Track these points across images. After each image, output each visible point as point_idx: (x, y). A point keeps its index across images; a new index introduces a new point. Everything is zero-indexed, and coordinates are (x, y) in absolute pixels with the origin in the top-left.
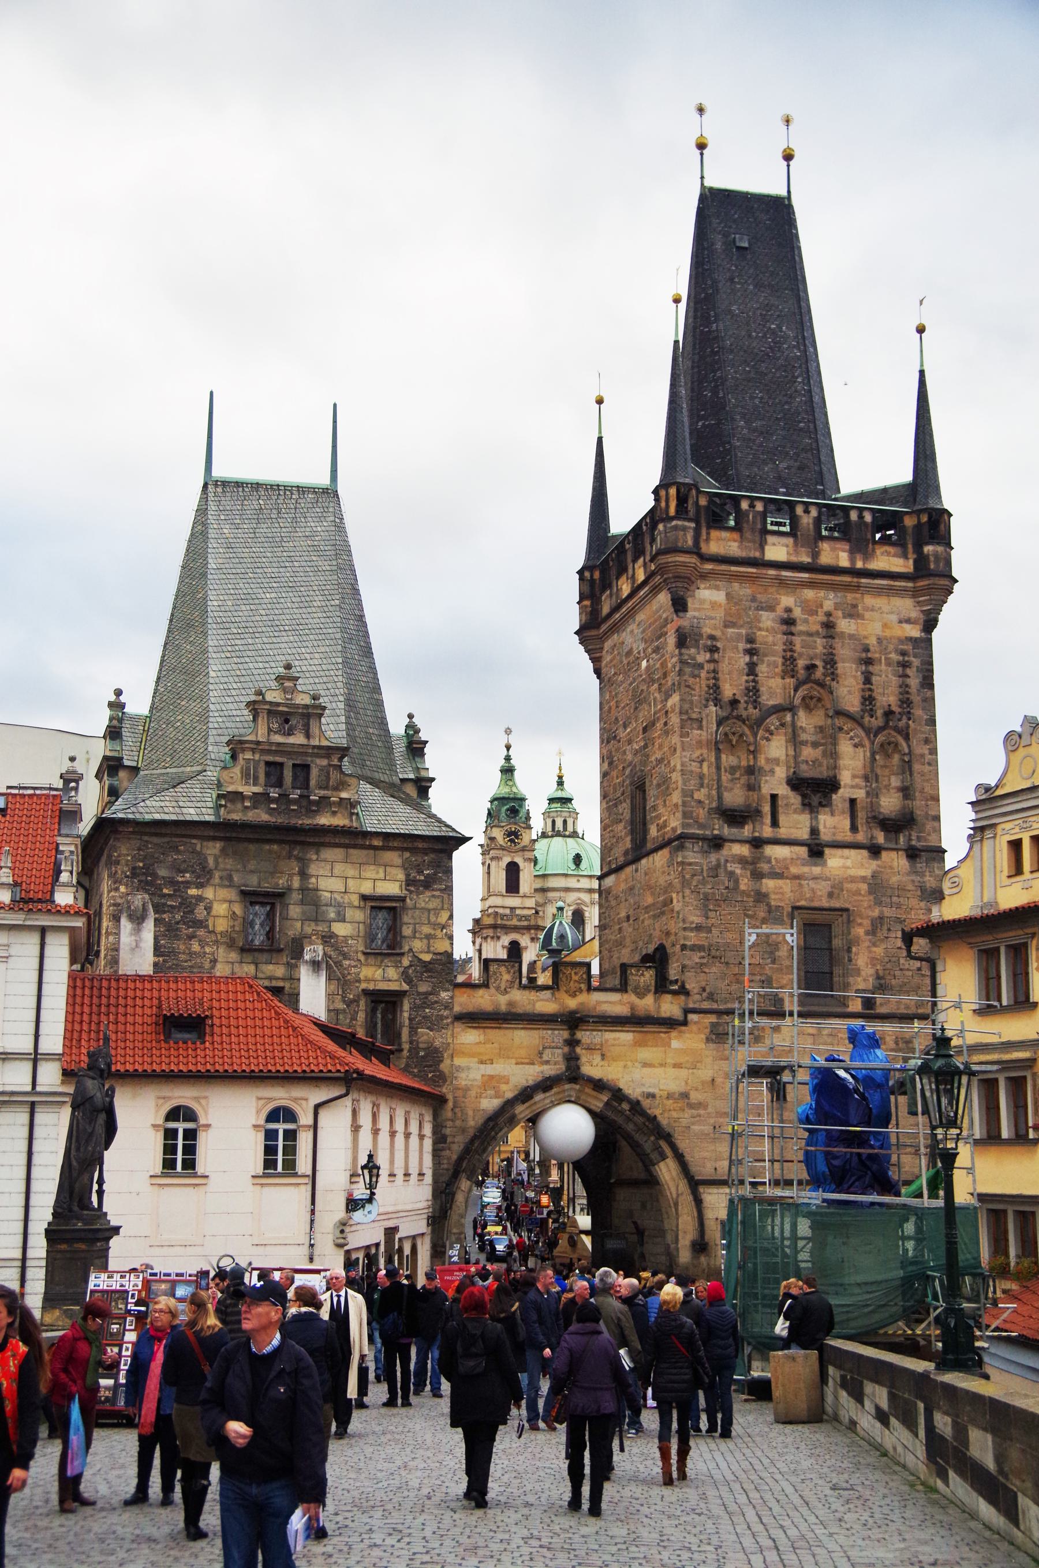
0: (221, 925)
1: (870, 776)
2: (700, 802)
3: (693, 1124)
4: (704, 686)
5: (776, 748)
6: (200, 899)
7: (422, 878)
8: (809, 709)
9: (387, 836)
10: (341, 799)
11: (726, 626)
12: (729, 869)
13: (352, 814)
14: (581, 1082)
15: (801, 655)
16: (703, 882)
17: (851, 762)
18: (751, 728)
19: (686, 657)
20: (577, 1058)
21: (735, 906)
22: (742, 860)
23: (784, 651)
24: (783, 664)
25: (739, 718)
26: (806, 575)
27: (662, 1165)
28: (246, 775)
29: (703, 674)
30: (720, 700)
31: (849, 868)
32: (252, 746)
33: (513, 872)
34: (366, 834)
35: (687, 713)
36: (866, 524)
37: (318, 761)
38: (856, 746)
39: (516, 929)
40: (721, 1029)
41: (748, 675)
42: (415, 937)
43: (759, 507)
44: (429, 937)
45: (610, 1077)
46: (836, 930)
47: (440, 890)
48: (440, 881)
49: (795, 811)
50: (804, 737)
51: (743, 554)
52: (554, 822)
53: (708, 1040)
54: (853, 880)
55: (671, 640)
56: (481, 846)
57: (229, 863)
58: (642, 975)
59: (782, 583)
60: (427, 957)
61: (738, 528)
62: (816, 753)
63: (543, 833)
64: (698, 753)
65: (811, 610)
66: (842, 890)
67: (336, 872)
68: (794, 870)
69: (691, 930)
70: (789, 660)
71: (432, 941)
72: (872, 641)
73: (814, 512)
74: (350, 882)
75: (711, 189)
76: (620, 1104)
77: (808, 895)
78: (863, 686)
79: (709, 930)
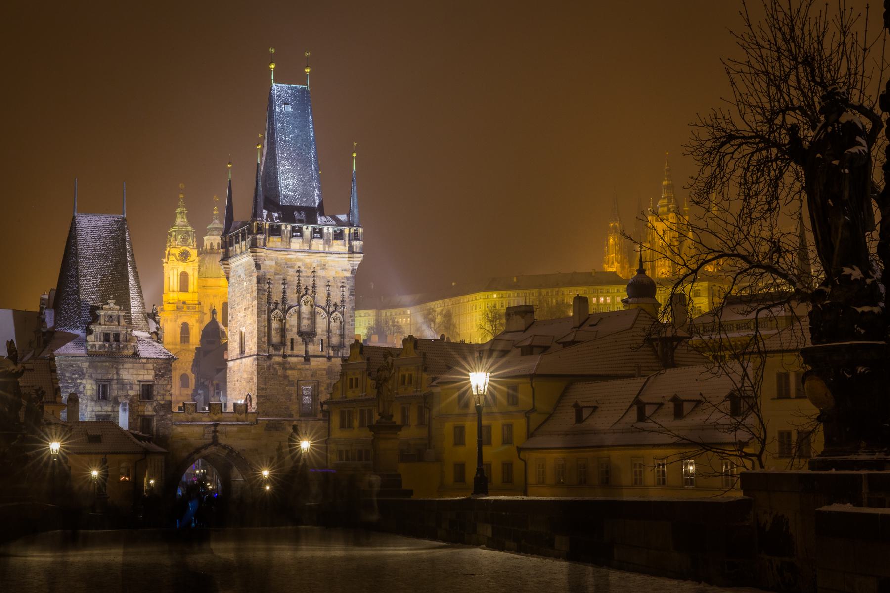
0: (89, 393)
1: (329, 331)
6: (81, 383)
9: (148, 358)
11: (276, 274)
17: (321, 324)
22: (279, 364)
28: (96, 337)
29: (266, 293)
43: (289, 228)
44: (163, 395)
50: (303, 316)
53: (265, 430)
54: (321, 369)
55: (255, 280)
57: (91, 370)
60: (162, 402)
68: (299, 367)
72: (331, 279)
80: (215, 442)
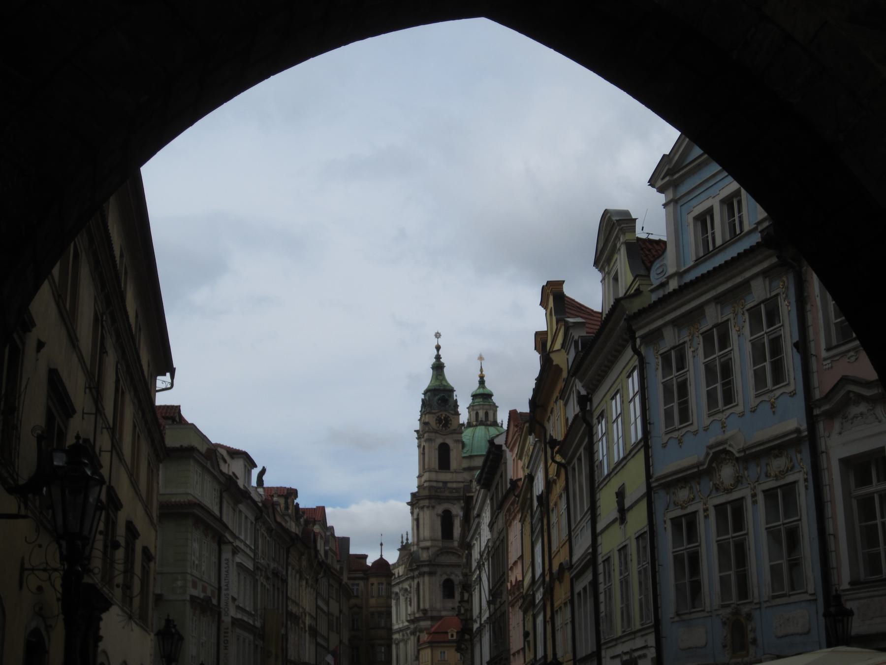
33: (444, 452)
39: (448, 499)
52: (477, 414)
56: (417, 431)
63: (469, 423)
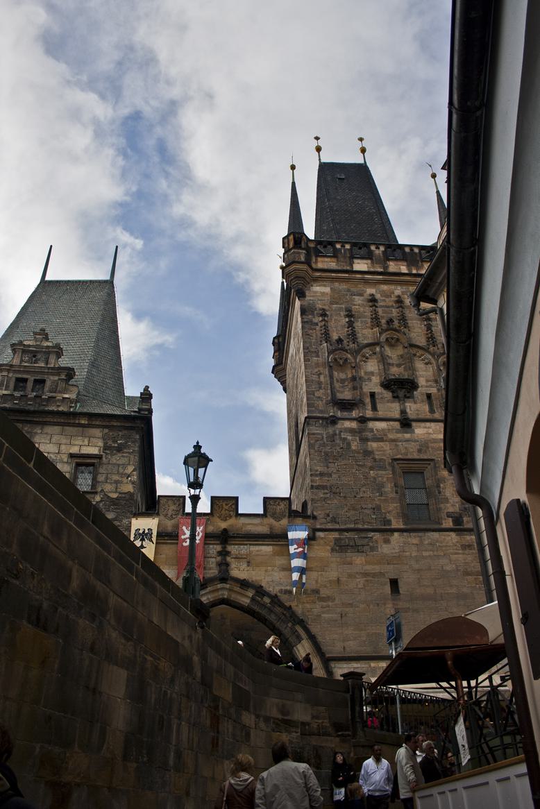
2: (319, 397)
3: (324, 613)
4: (319, 334)
5: (372, 366)
7: (116, 445)
8: (392, 346)
10: (63, 398)
11: (332, 303)
12: (343, 436)
13: (71, 407)
14: (233, 583)
15: (383, 317)
16: (324, 445)
18: (352, 354)
19: (305, 320)
20: (227, 565)
21: (349, 460)
22: (352, 431)
23: (372, 315)
24: (371, 322)
25: (343, 350)
26: (381, 277)
27: (299, 646)
29: (318, 328)
30: (330, 341)
31: (430, 434)
32: (7, 368)
34: (75, 415)
35: (308, 348)
36: (416, 253)
37: (52, 378)
38: (427, 364)
40: (343, 542)
41: (348, 328)
42: (107, 482)
43: (348, 247)
44: (117, 482)
45: (254, 579)
46: (427, 474)
47: (129, 453)
48: (129, 447)
49: (388, 402)
50: (390, 361)
51: (340, 268)
53: (333, 550)
54: (435, 441)
58: (279, 504)
59: (367, 282)
60: (114, 496)
61: (335, 256)
62: (401, 369)
64: (316, 370)
65: (387, 295)
66: (428, 448)
67: (53, 440)
68: (391, 436)
69: (316, 475)
70: (376, 321)
71: (119, 485)
73: (382, 248)
74: (63, 447)
75: (324, 163)
76: (262, 599)
77: (403, 452)
78: (425, 332)
79: (331, 475)
80: (224, 577)
